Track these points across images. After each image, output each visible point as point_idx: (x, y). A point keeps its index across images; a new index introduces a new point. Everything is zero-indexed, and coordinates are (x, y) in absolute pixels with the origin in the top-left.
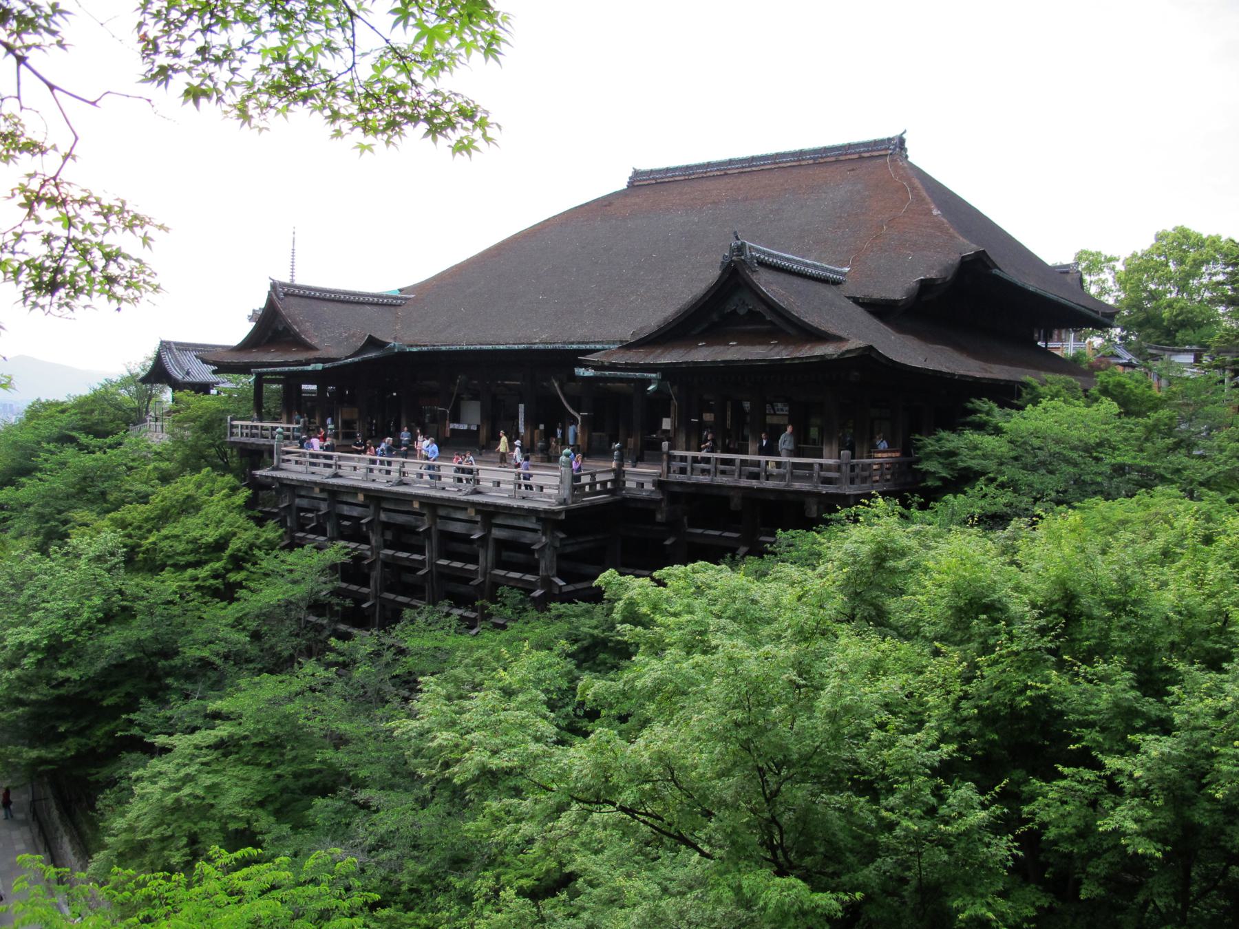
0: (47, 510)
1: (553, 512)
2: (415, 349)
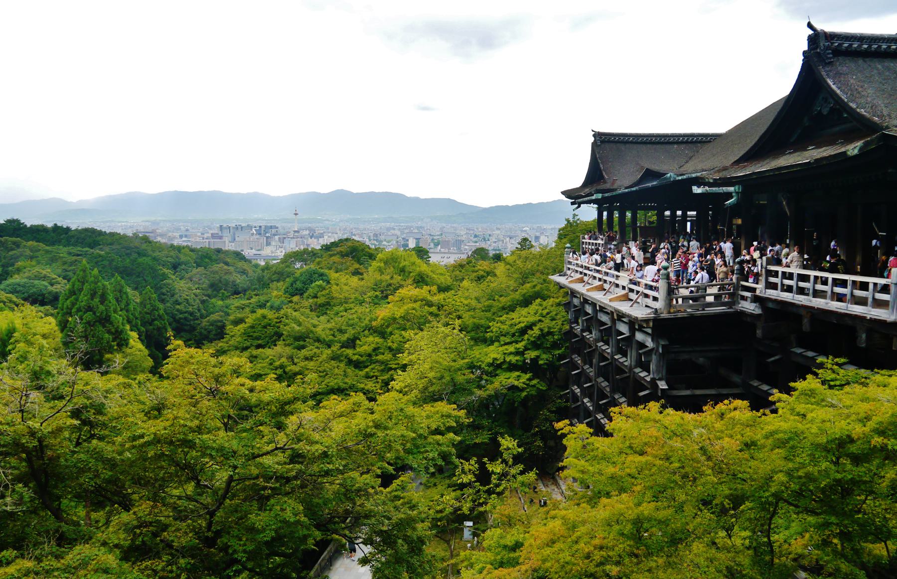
2: (680, 178)
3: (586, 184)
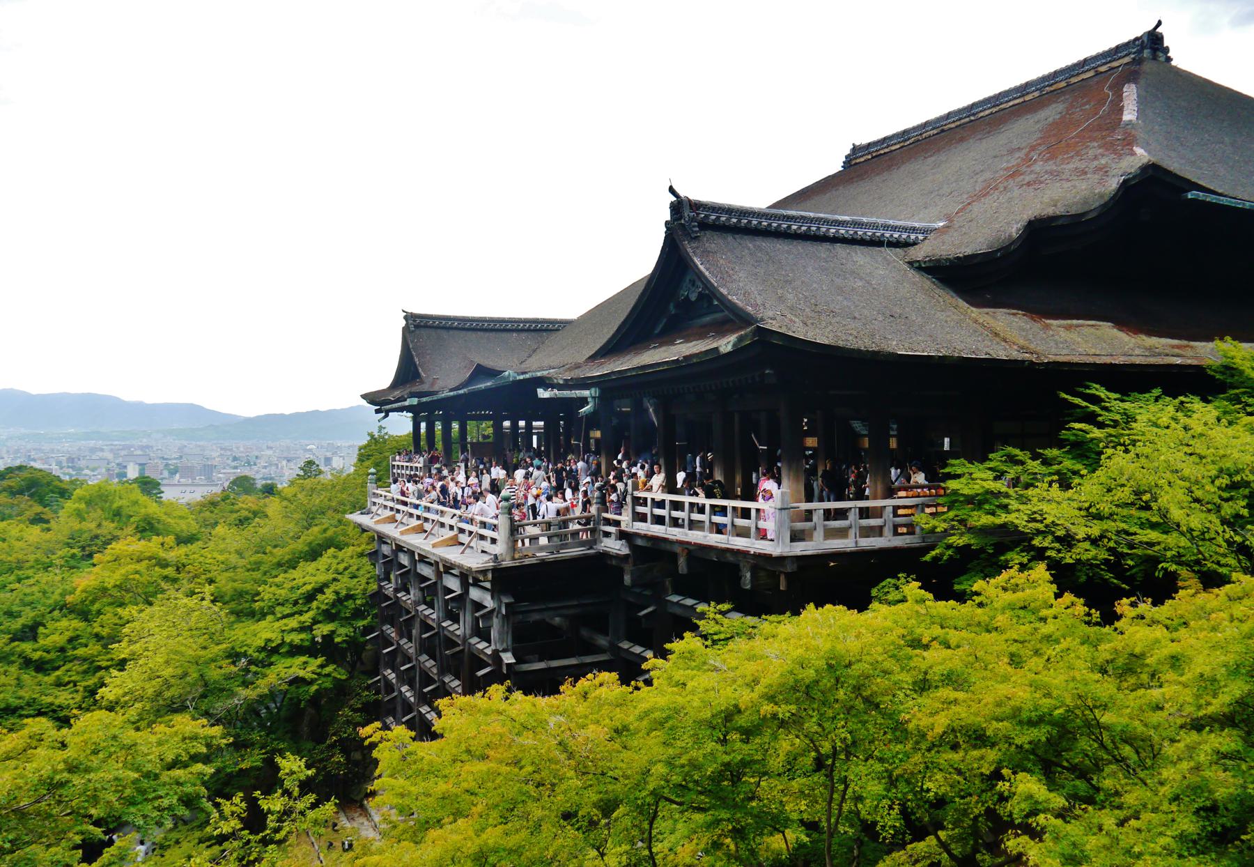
2: (521, 377)
3: (395, 385)
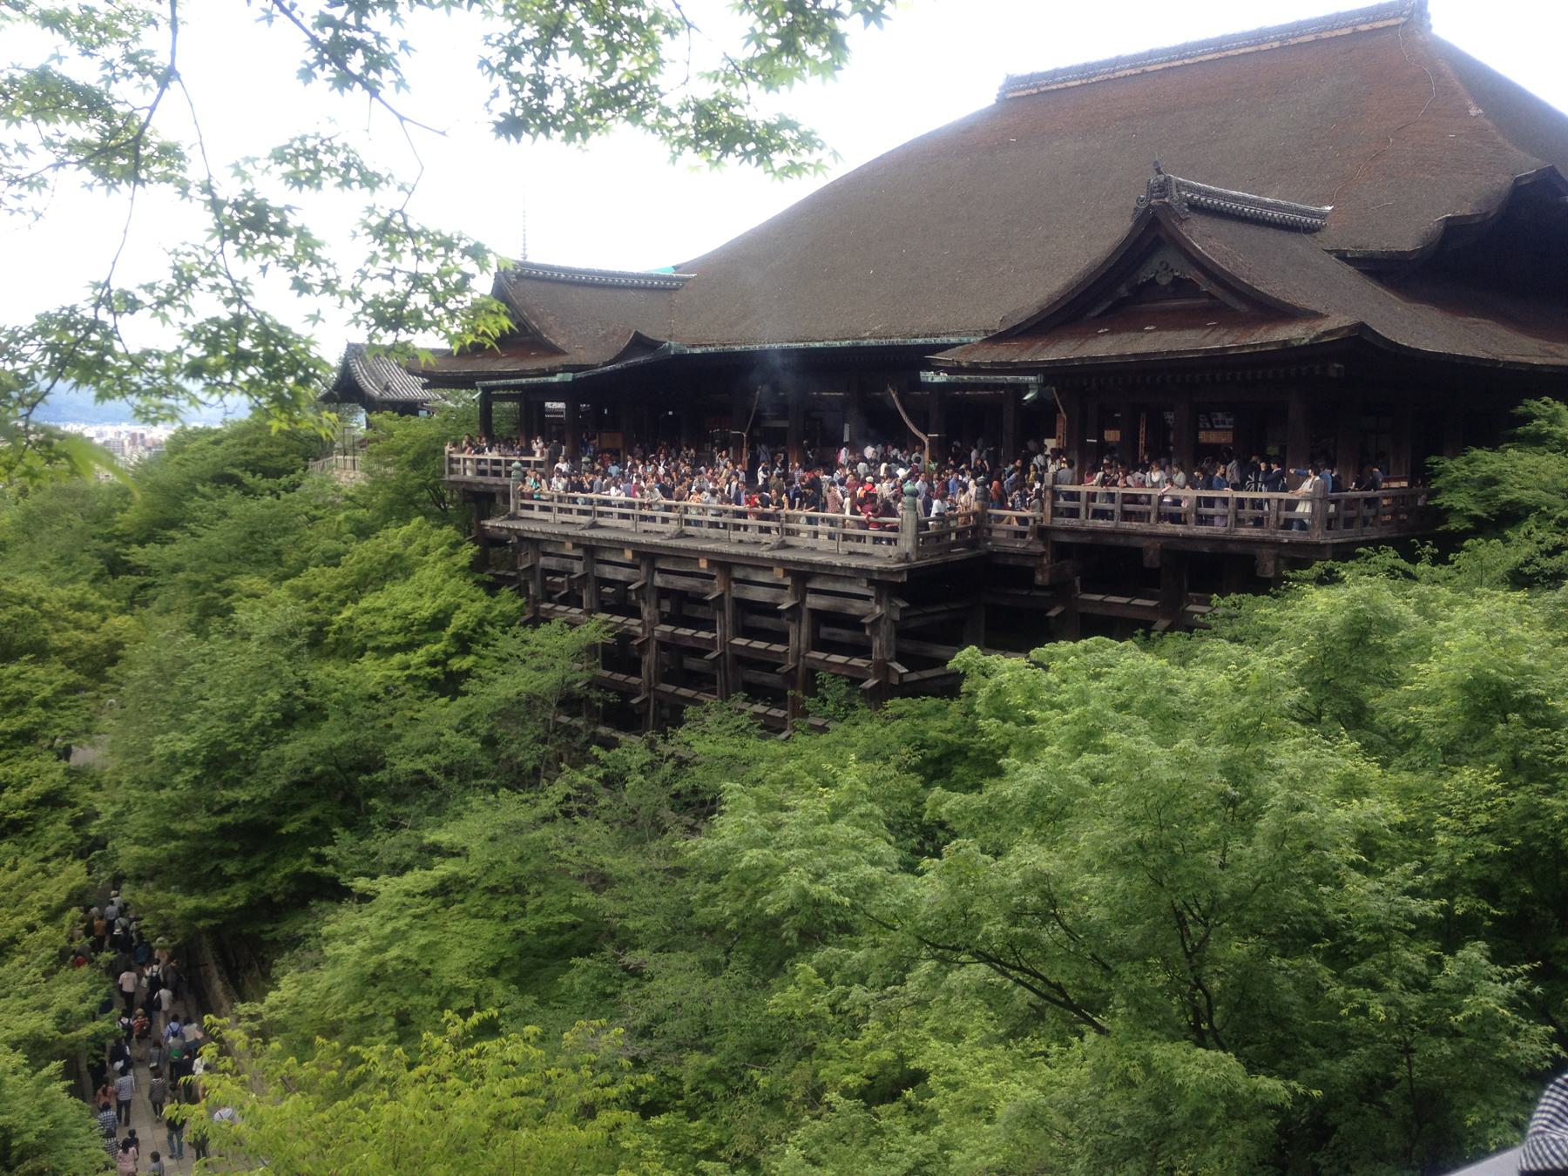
0: (202, 577)
1: (891, 572)
2: (698, 351)
